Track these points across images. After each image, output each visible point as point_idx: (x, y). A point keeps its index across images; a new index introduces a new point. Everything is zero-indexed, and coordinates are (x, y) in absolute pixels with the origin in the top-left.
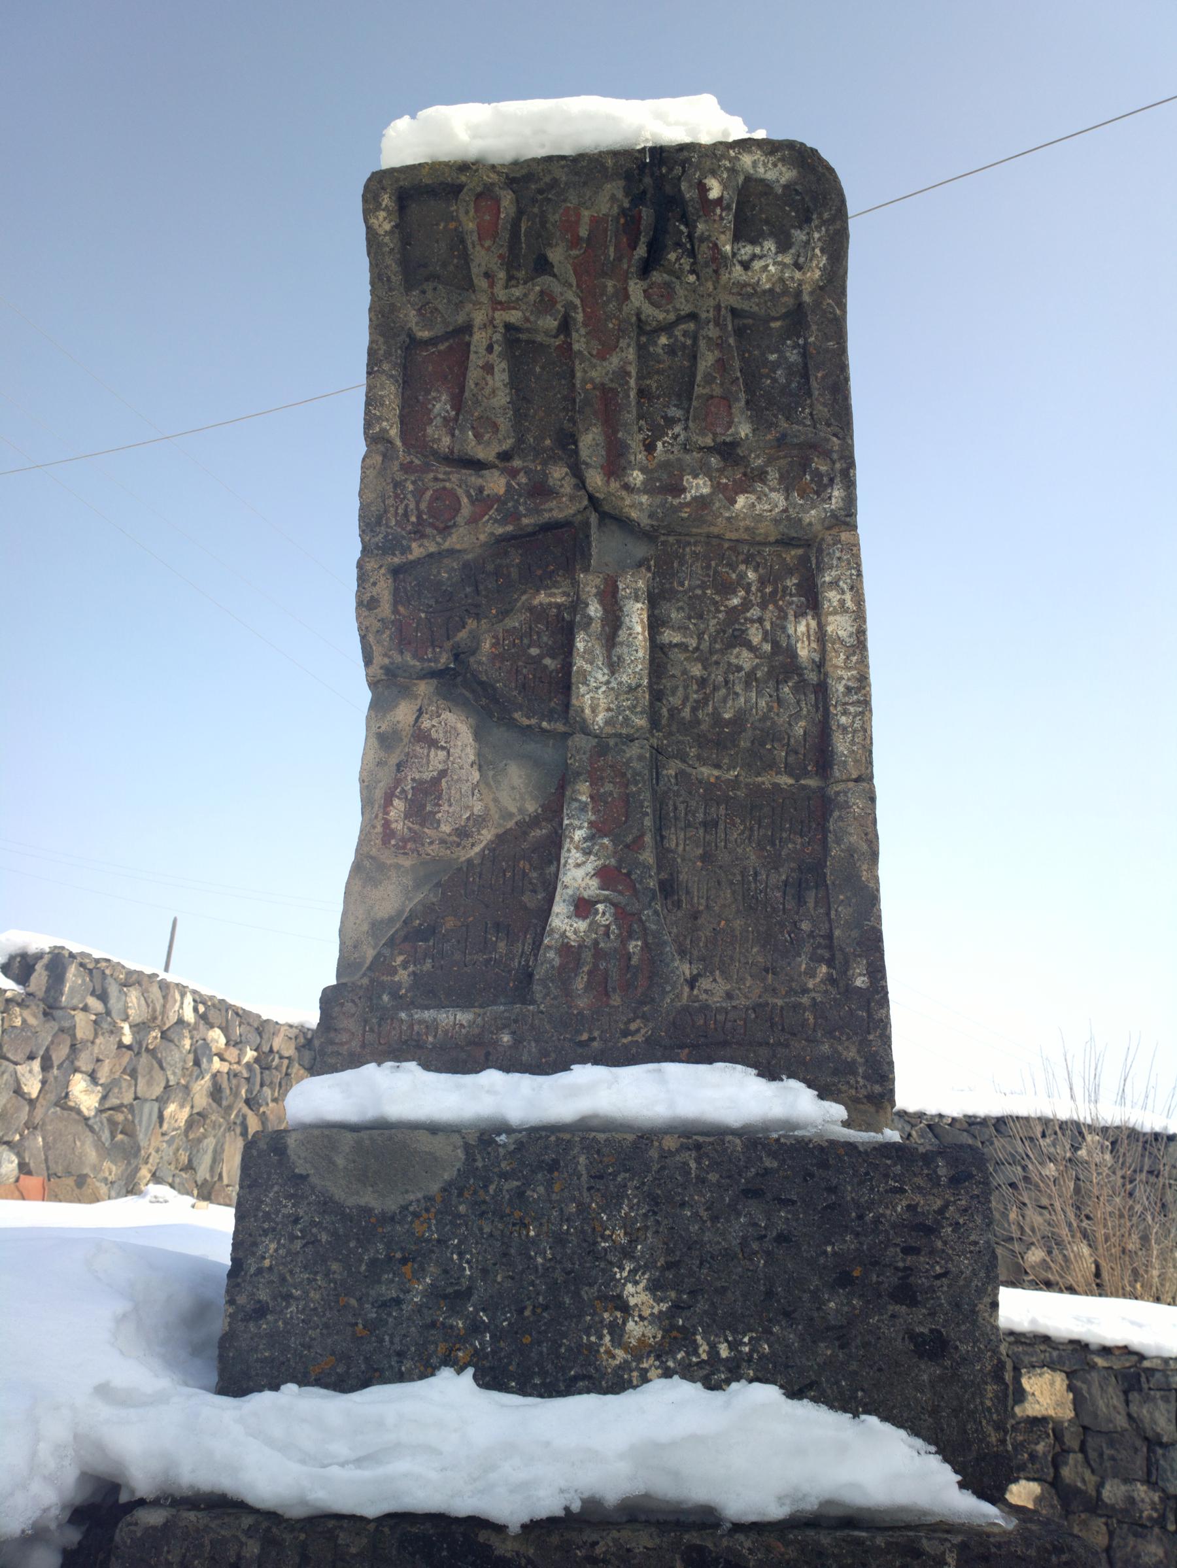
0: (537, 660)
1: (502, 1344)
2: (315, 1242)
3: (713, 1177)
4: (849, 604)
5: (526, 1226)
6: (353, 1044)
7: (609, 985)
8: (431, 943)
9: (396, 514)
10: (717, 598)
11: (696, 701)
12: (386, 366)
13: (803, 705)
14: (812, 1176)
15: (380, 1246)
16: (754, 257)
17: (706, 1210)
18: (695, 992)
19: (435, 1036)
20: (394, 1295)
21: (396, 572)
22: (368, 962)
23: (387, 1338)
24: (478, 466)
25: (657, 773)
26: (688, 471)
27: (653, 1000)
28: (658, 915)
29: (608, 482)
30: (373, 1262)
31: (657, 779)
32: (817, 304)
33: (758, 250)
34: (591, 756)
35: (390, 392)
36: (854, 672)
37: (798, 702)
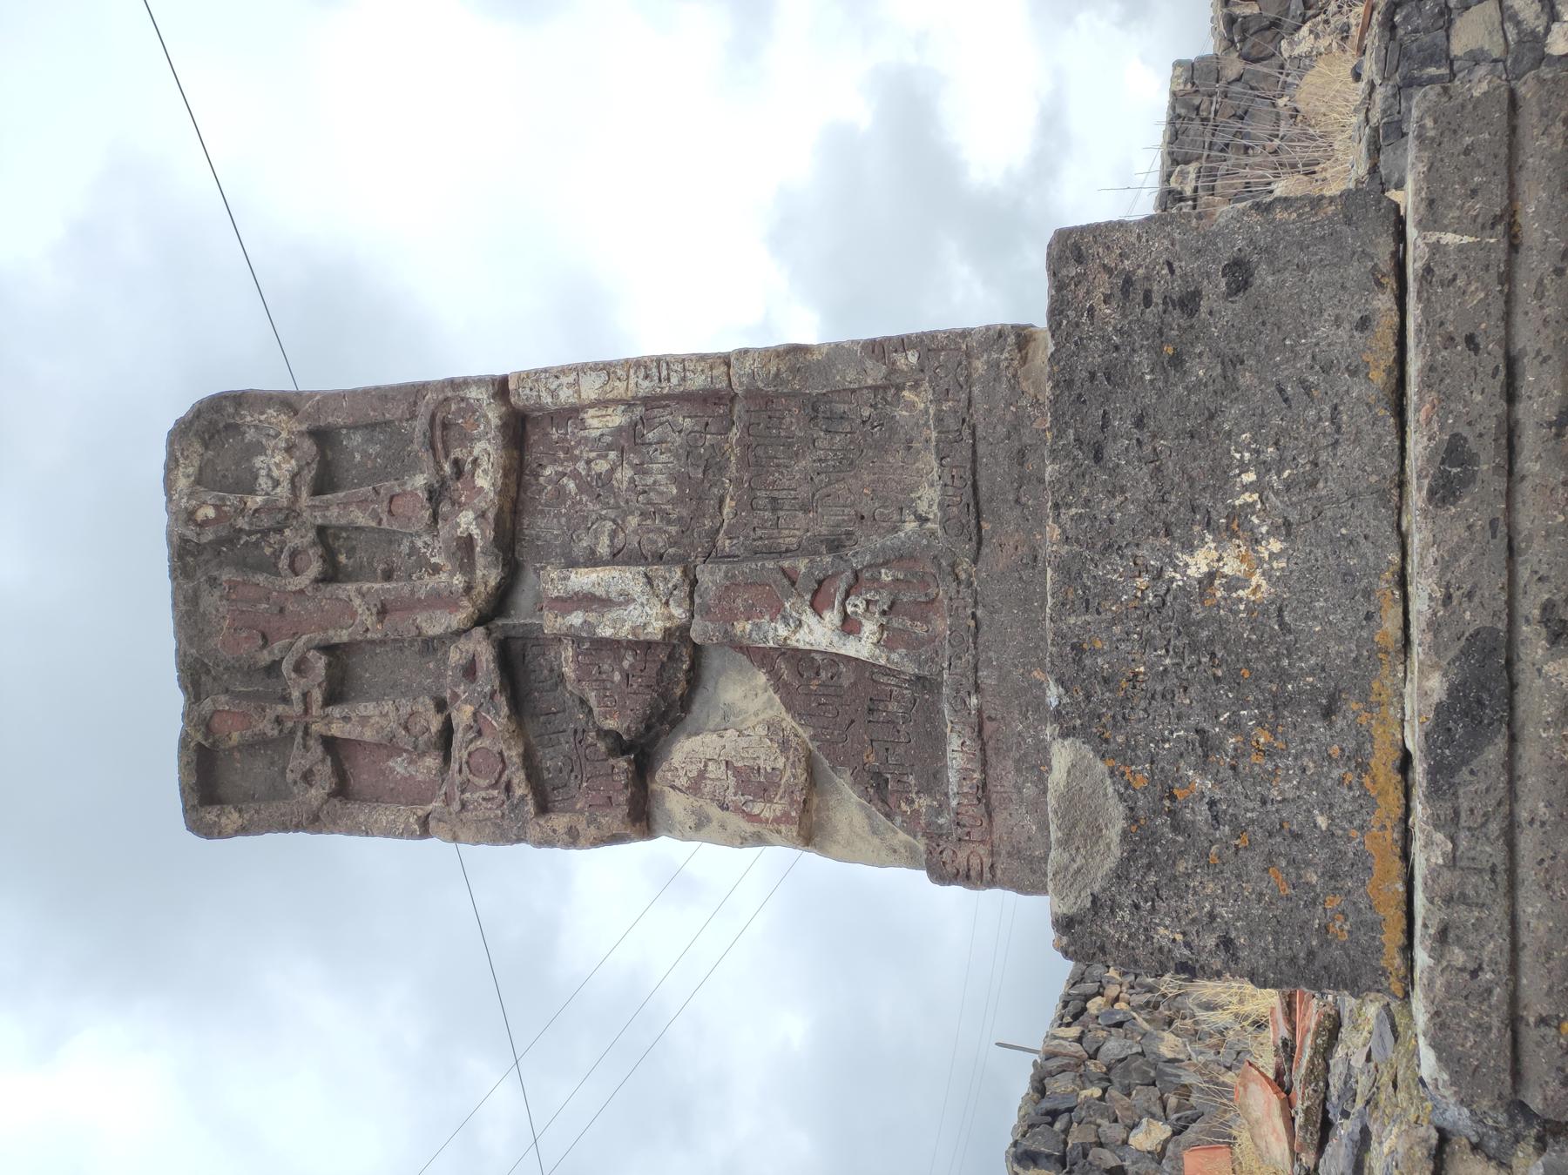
0: (627, 676)
1: (1251, 698)
2: (1157, 888)
3: (1086, 492)
4: (571, 379)
5: (1136, 675)
6: (982, 852)
7: (923, 599)
8: (889, 776)
9: (490, 809)
10: (569, 502)
11: (661, 521)
12: (362, 818)
13: (664, 419)
14: (1080, 395)
15: (1158, 822)
16: (269, 476)
17: (1114, 497)
18: (931, 516)
19: (974, 771)
20: (1207, 807)
21: (543, 808)
22: (910, 839)
23: (1249, 815)
24: (447, 731)
25: (729, 557)
26: (453, 532)
27: (935, 557)
28: (857, 553)
29: (464, 608)
30: (1176, 828)
31: (735, 557)
32: (308, 416)
33: (263, 472)
34: (710, 621)
35: (384, 816)
36: (632, 371)
37: (661, 424)
